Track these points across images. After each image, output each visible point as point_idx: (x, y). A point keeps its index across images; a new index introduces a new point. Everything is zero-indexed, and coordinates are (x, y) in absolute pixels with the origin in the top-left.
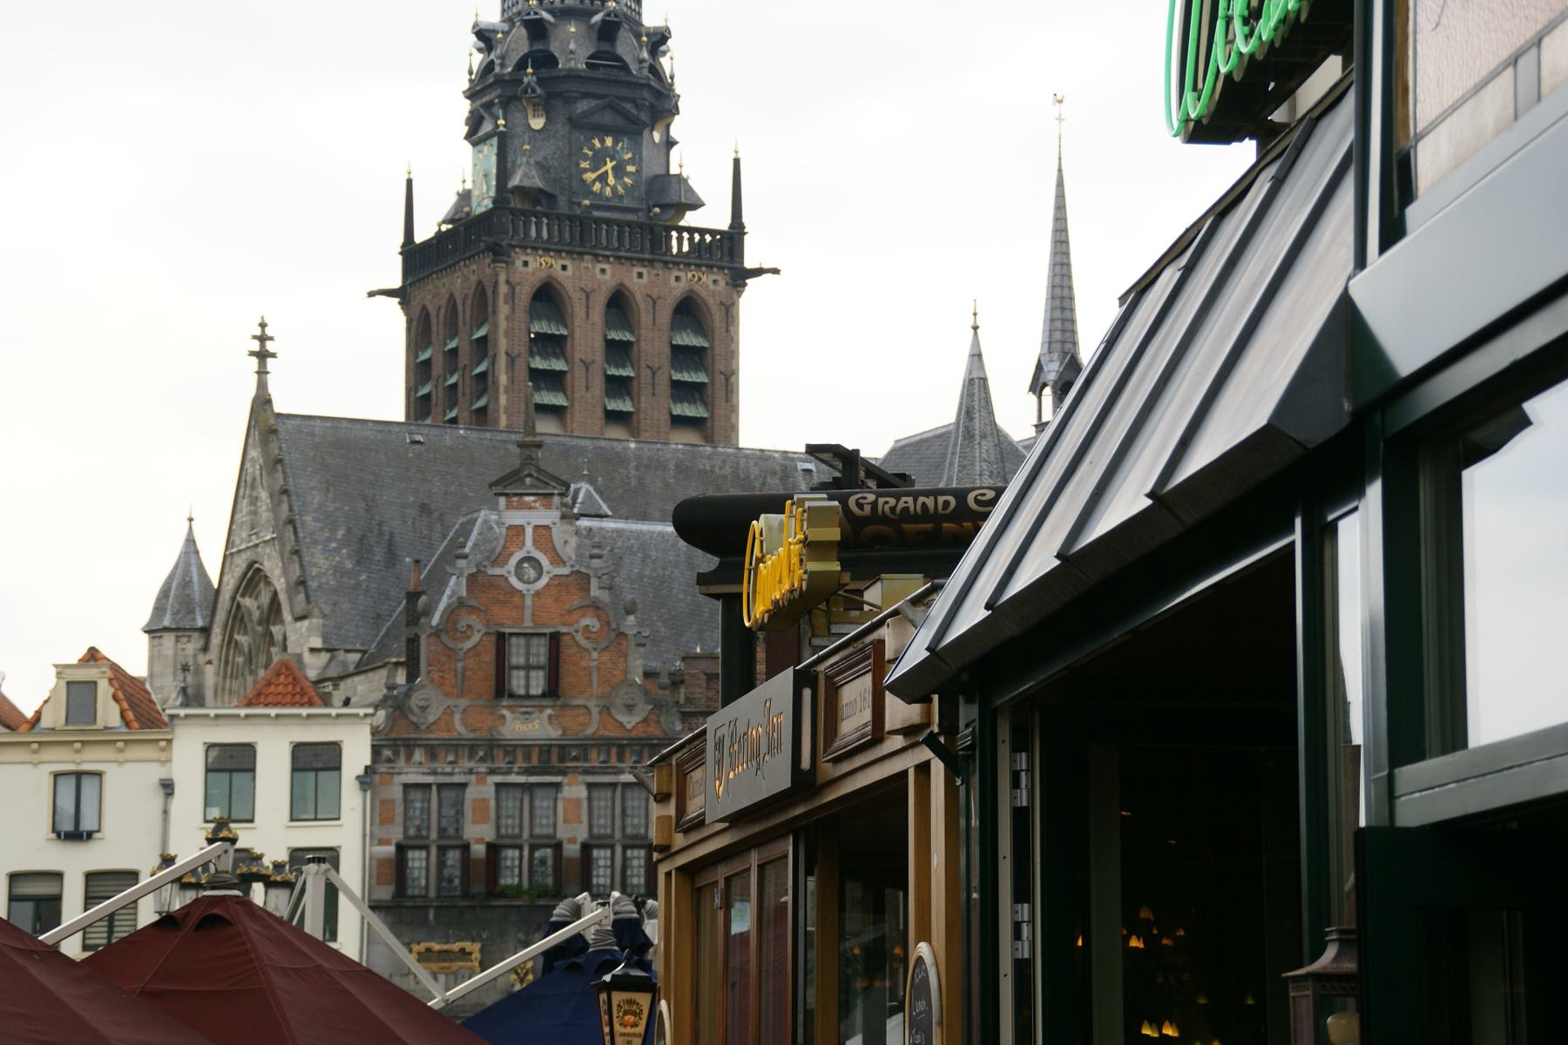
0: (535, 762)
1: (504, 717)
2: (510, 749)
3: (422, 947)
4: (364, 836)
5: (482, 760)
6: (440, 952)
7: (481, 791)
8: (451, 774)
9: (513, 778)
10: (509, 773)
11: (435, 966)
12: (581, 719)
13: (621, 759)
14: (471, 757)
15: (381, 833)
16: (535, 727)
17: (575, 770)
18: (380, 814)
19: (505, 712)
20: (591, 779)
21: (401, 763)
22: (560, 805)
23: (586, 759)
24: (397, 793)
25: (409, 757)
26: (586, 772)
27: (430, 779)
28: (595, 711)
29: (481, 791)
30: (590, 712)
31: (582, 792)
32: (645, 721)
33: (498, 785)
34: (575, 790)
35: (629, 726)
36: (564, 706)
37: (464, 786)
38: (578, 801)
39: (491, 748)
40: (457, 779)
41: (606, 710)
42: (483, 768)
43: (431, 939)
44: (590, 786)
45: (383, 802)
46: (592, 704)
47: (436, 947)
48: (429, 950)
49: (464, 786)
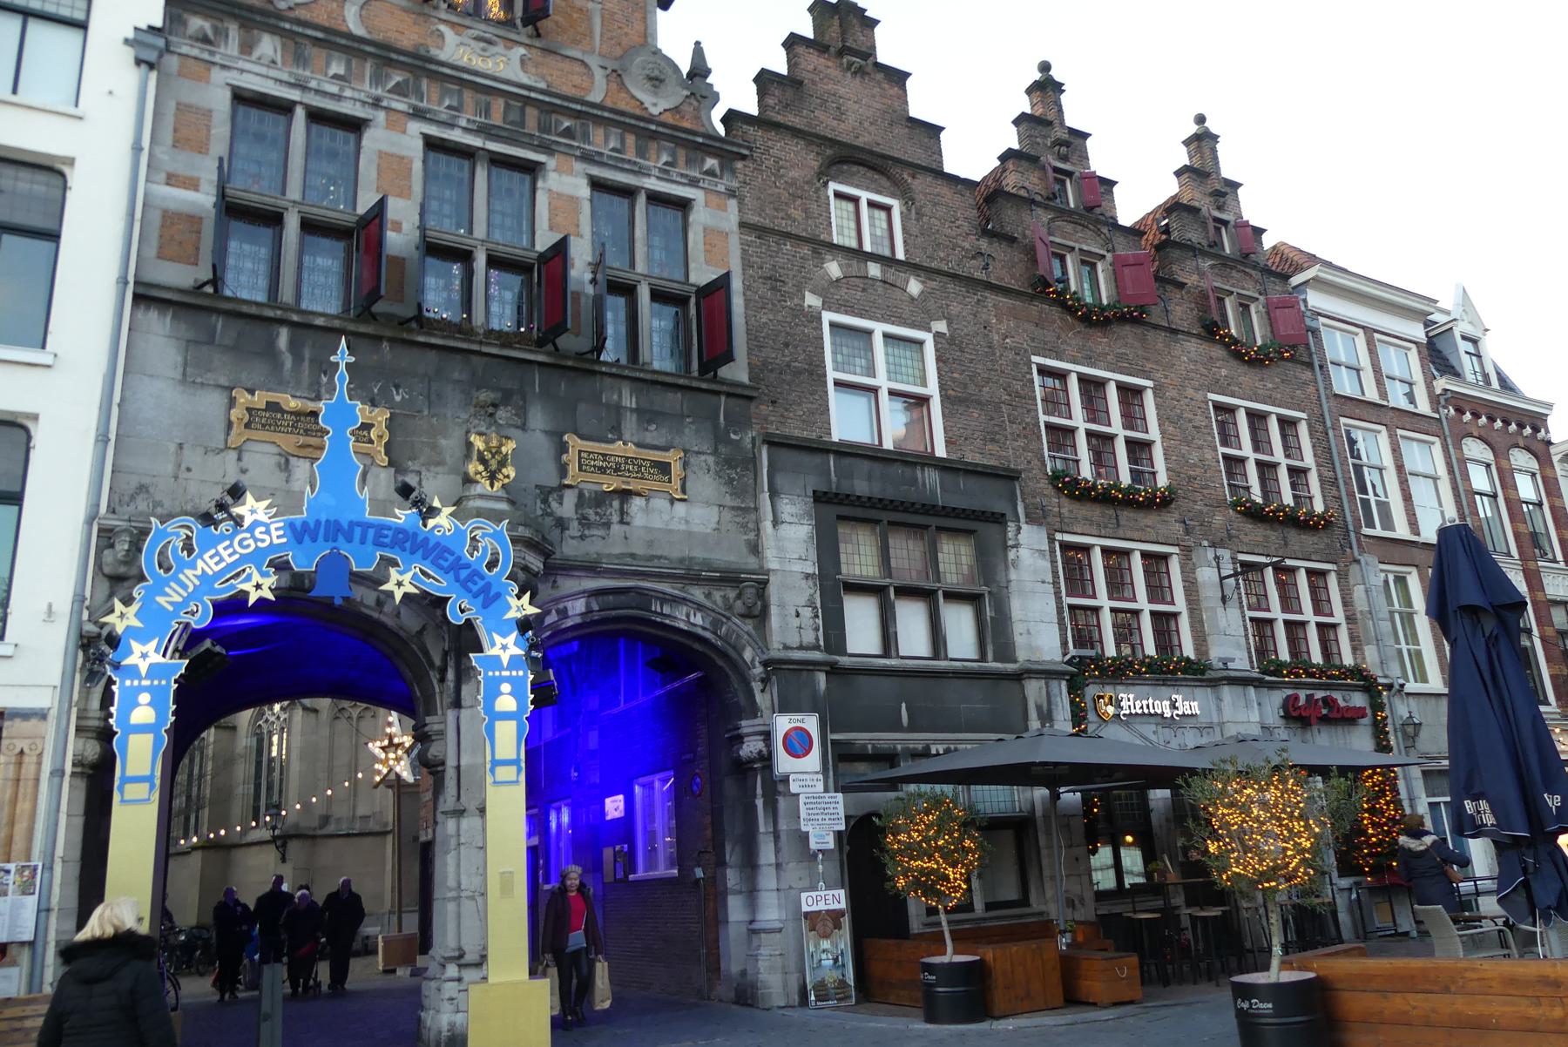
0: (497, 119)
1: (442, 36)
2: (459, 80)
3: (260, 399)
4: (137, 148)
5: (399, 90)
6: (297, 414)
7: (393, 141)
8: (338, 97)
9: (456, 135)
10: (452, 126)
11: (289, 442)
12: (577, 80)
13: (641, 153)
14: (377, 80)
15: (174, 161)
16: (507, 64)
17: (568, 152)
18: (172, 127)
19: (442, 28)
20: (596, 171)
21: (232, 47)
22: (541, 198)
23: (586, 138)
24: (220, 101)
25: (247, 48)
26: (587, 158)
27: (294, 95)
28: (599, 75)
29: (393, 141)
30: (591, 75)
31: (584, 191)
32: (676, 110)
33: (431, 144)
34: (565, 182)
35: (655, 111)
36: (548, 51)
37: (355, 126)
38: (574, 200)
39: (421, 66)
40: (346, 108)
41: (617, 76)
42: (400, 105)
43: (281, 385)
44: (597, 185)
45: (182, 108)
46: (594, 62)
47: (293, 404)
48: (273, 407)
49: (355, 126)
